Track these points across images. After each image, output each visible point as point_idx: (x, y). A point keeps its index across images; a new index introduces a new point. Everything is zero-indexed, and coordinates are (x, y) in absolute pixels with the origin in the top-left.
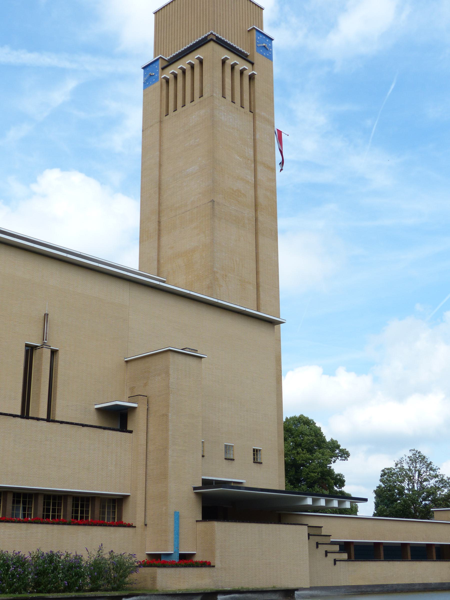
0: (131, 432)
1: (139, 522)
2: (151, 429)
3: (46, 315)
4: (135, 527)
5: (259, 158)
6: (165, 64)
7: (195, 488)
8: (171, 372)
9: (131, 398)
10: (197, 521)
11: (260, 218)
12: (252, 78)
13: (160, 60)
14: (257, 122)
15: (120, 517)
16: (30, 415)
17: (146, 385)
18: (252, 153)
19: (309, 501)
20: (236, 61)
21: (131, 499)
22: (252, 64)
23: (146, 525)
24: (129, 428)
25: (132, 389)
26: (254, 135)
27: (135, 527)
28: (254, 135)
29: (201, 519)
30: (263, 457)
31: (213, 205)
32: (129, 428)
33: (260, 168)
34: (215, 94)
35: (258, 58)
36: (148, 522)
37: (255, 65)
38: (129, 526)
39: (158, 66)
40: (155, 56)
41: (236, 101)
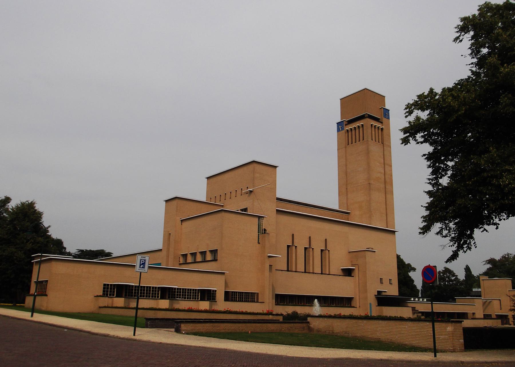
0: (353, 276)
1: (358, 306)
2: (360, 276)
3: (326, 240)
4: (356, 307)
5: (386, 162)
6: (347, 123)
7: (375, 295)
8: (367, 257)
9: (352, 265)
10: (376, 306)
11: (387, 187)
12: (382, 129)
13: (344, 122)
14: (385, 148)
15: (351, 304)
16: (323, 273)
17: (357, 260)
18: (383, 161)
19: (412, 299)
20: (376, 124)
21: (354, 299)
22: (382, 123)
23: (360, 307)
24: (352, 275)
25: (352, 261)
26: (384, 153)
27: (356, 307)
28: (384, 153)
29: (377, 305)
30: (392, 282)
31: (370, 185)
32: (352, 275)
33: (386, 166)
34: (369, 140)
35: (384, 120)
36: (360, 306)
37: (383, 123)
38: (354, 307)
39: (343, 124)
40: (341, 119)
41: (376, 141)
